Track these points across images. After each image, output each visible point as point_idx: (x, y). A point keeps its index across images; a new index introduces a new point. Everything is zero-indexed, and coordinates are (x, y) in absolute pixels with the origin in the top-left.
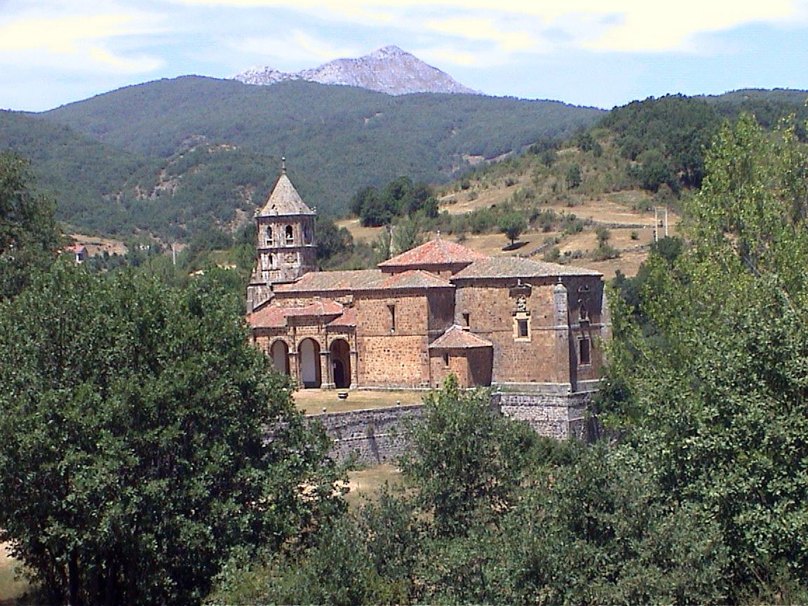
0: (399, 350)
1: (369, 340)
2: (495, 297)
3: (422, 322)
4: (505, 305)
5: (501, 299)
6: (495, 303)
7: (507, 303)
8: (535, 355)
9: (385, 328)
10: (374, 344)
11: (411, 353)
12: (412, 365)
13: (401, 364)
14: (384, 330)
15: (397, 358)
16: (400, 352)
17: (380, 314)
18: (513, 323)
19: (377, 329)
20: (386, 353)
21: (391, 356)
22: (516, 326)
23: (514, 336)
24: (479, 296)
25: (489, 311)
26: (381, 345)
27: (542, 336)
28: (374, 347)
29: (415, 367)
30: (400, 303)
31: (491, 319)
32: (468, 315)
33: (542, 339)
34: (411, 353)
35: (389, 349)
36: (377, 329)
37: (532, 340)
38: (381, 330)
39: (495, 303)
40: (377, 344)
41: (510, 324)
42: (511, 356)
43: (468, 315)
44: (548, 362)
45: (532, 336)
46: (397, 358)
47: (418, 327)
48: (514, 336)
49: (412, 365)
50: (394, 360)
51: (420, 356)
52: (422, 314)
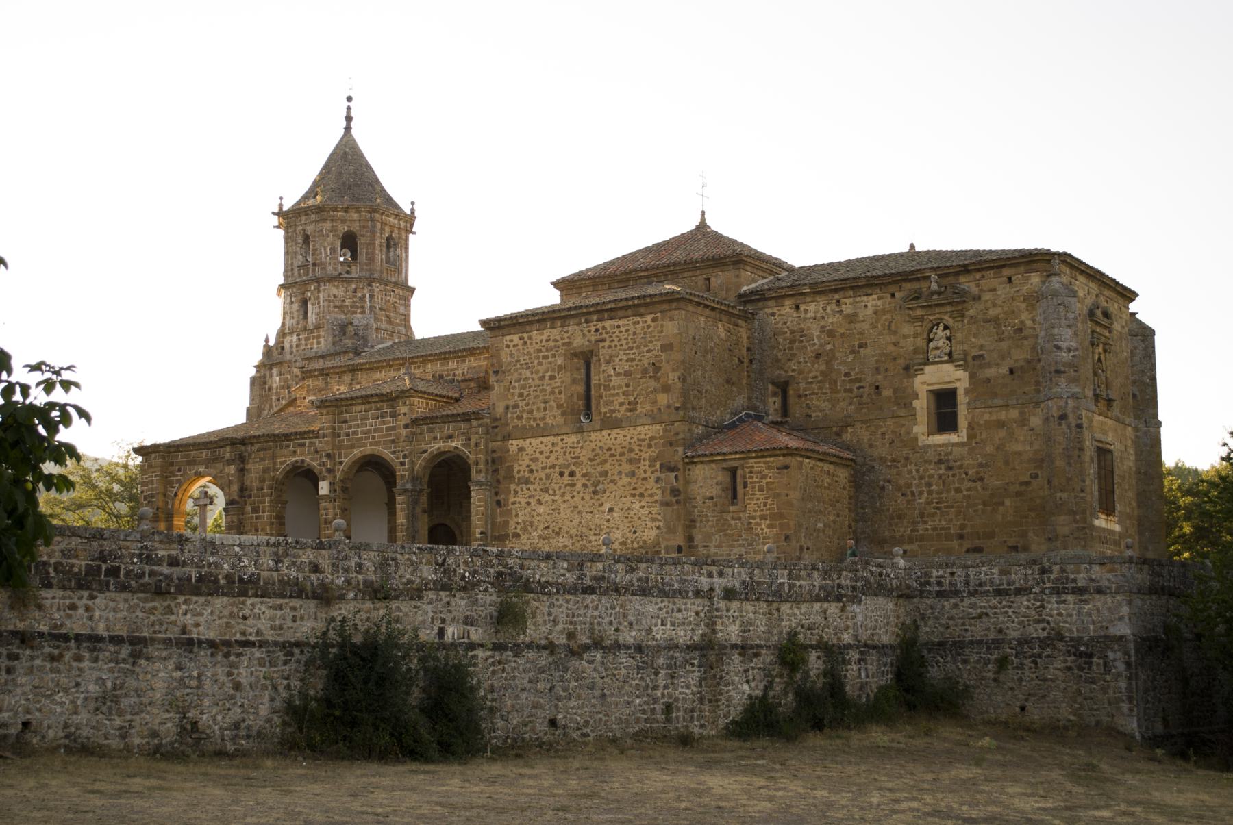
0: (599, 469)
1: (521, 449)
2: (861, 333)
3: (666, 389)
4: (891, 348)
5: (881, 334)
6: (860, 346)
7: (895, 344)
8: (982, 479)
9: (564, 414)
10: (536, 460)
11: (633, 474)
12: (637, 506)
13: (607, 506)
14: (560, 420)
15: (595, 492)
16: (604, 474)
17: (552, 378)
18: (916, 396)
19: (543, 419)
20: (566, 479)
21: (579, 486)
22: (921, 405)
23: (916, 429)
24: (817, 333)
25: (844, 369)
26: (552, 460)
27: (1001, 424)
28: (533, 467)
29: (645, 512)
30: (607, 344)
31: (850, 391)
32: (787, 383)
33: (1002, 433)
34: (633, 474)
35: (573, 468)
36: (543, 419)
37: (970, 437)
38: (554, 418)
39: (860, 346)
40: (542, 457)
41: (904, 399)
42: (909, 485)
43: (787, 383)
44: (1019, 494)
45: (971, 427)
46: (595, 492)
47: (654, 402)
48: (916, 429)
49: (637, 506)
50: (587, 498)
51: (658, 480)
52: (666, 367)
